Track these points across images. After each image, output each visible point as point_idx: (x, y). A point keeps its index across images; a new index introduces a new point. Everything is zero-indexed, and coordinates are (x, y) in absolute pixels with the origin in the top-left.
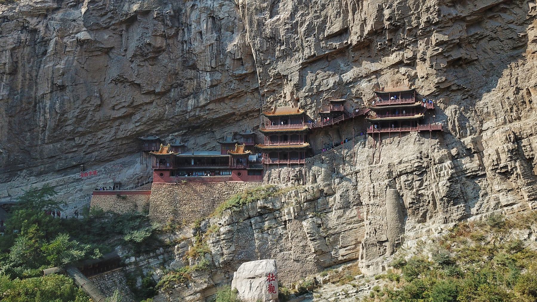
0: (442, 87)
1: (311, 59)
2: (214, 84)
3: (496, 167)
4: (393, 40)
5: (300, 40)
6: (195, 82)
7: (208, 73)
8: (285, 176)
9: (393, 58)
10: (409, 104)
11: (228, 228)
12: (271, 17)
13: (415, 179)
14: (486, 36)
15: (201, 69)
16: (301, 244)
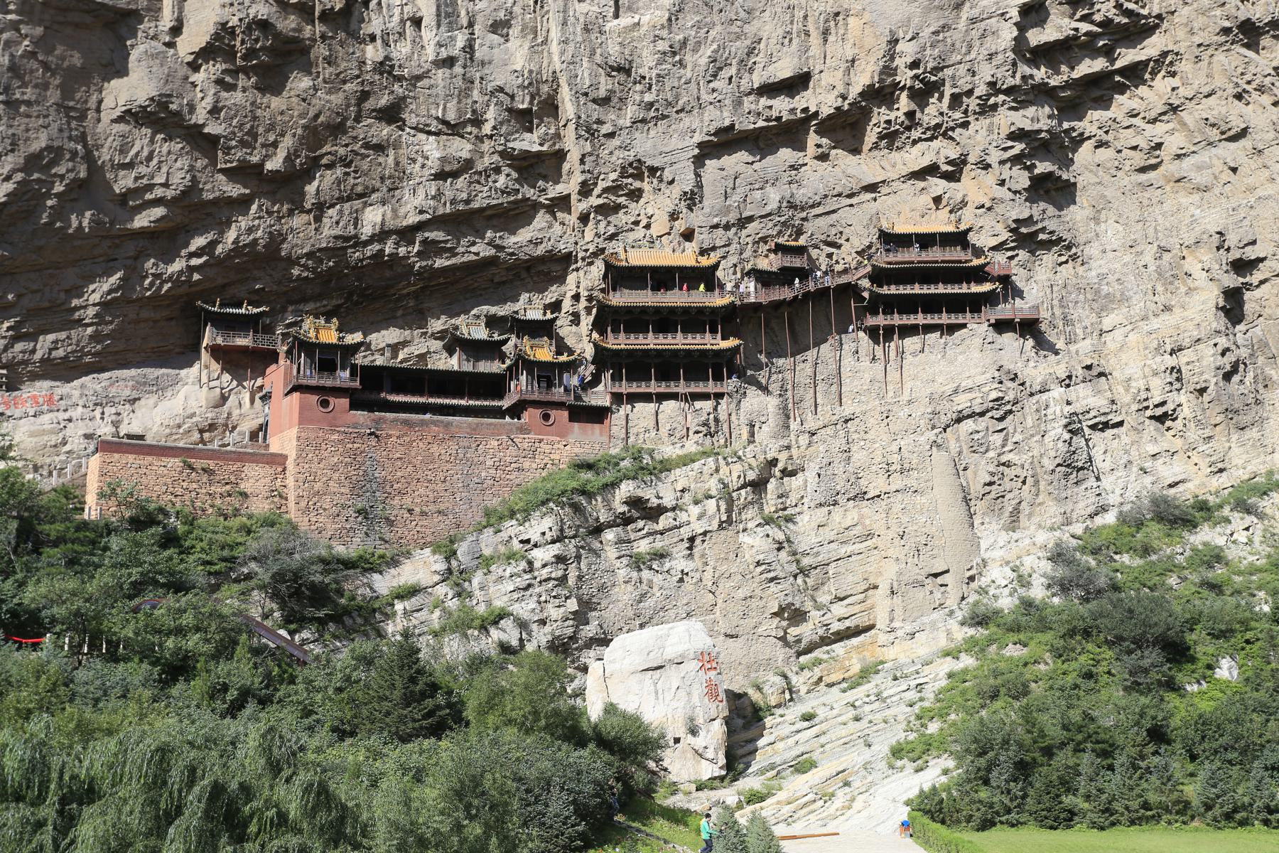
0: (1024, 230)
1: (724, 137)
2: (447, 169)
3: (1145, 404)
4: (918, 115)
5: (693, 86)
6: (391, 160)
7: (432, 138)
8: (675, 425)
9: (917, 157)
10: (960, 262)
11: (556, 549)
12: (616, 16)
13: (991, 430)
14: (1089, 138)
15: (411, 120)
16: (741, 594)
